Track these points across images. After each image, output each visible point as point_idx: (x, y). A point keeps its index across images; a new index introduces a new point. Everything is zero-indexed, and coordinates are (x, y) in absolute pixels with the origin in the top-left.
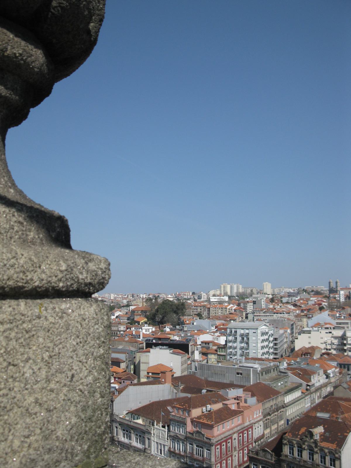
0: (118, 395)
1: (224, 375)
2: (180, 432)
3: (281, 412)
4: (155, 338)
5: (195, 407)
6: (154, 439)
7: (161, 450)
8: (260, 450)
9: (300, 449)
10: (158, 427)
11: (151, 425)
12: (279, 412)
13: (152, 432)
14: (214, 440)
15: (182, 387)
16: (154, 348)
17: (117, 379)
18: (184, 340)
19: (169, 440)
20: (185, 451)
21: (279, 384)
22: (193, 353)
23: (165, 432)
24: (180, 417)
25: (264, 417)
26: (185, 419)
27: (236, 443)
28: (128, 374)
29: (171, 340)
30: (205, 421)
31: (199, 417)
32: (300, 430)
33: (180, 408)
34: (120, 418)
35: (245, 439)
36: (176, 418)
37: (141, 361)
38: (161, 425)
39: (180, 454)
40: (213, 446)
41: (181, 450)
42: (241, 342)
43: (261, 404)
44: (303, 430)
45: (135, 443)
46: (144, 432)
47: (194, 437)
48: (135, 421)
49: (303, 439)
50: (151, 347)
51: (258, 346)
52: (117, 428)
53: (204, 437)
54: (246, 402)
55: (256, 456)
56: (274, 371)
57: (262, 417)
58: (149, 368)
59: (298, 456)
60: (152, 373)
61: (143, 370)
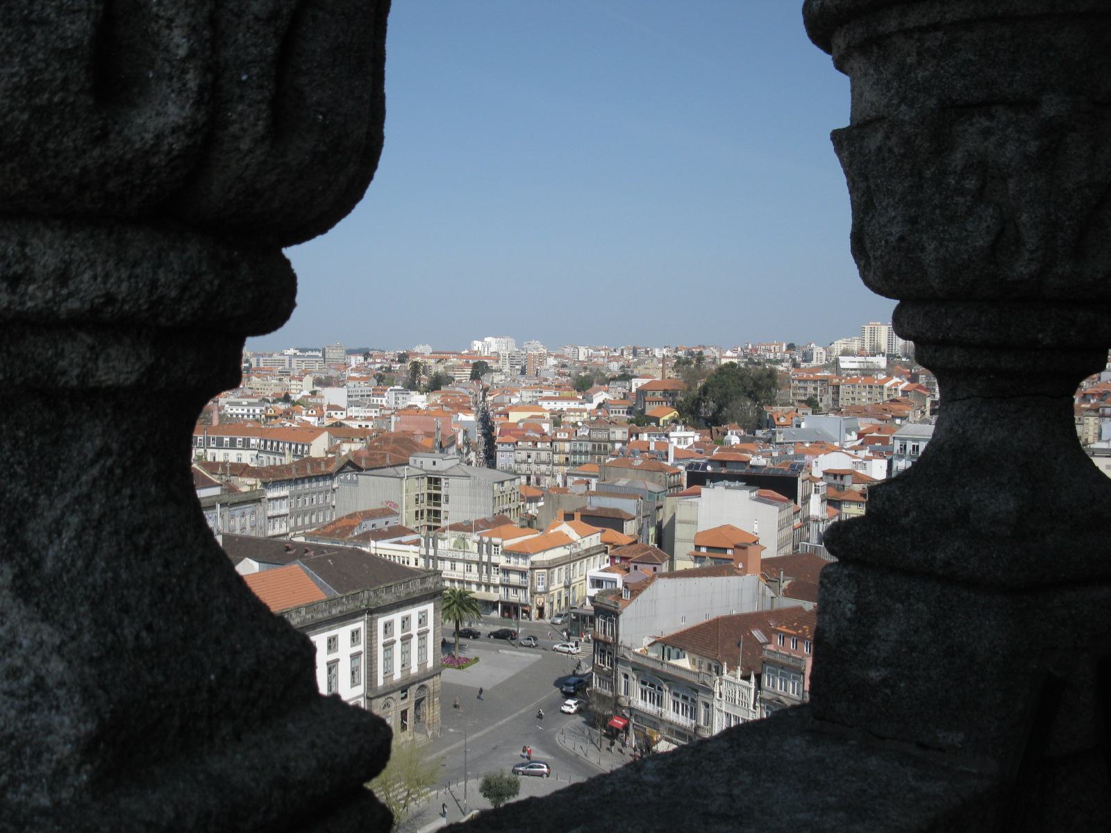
4: (711, 462)
10: (732, 679)
11: (715, 674)
13: (717, 690)
15: (787, 583)
17: (617, 561)
18: (786, 468)
19: (758, 710)
22: (806, 499)
23: (749, 689)
24: (789, 656)
26: (801, 660)
28: (647, 549)
29: (752, 467)
33: (790, 635)
34: (636, 654)
37: (678, 517)
38: (739, 673)
46: (695, 689)
48: (673, 662)
50: (703, 484)
52: (626, 676)
61: (682, 540)
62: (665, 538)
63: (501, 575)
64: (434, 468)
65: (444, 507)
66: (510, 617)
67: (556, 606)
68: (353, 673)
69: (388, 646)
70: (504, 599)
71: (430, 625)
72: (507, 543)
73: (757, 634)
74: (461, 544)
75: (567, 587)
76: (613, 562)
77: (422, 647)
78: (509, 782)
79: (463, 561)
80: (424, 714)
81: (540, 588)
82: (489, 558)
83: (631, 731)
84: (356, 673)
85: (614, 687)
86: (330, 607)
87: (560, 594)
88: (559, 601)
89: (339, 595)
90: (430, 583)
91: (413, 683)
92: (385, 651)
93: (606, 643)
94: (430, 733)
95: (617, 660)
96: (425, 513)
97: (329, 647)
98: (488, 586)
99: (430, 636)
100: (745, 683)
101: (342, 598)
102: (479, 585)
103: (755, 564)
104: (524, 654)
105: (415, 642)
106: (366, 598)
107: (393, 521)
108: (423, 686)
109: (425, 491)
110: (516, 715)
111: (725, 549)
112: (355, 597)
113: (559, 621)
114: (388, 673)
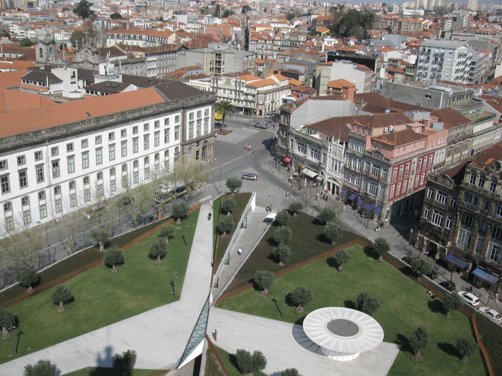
0: (296, 109)
1: (411, 96)
2: (358, 150)
3: (467, 141)
4: (338, 51)
5: (377, 126)
6: (330, 155)
7: (336, 166)
8: (440, 176)
9: (482, 179)
10: (335, 144)
12: (465, 141)
13: (329, 148)
14: (392, 162)
15: (364, 105)
16: (337, 61)
17: (294, 92)
18: (371, 56)
19: (346, 157)
20: (361, 170)
21: (471, 112)
22: (379, 70)
23: (342, 148)
24: (360, 135)
25: (449, 144)
26: (365, 137)
27: (414, 167)
28: (307, 88)
29: (356, 54)
30: (386, 142)
31: (380, 137)
32: (486, 160)
34: (297, 131)
35: (425, 164)
36: (355, 136)
37: (322, 75)
38: (339, 141)
39: (355, 172)
40: (391, 166)
41: (357, 168)
42: (434, 63)
43: (447, 130)
44: (490, 161)
45: (310, 158)
46: (320, 147)
47: (372, 156)
48: (311, 135)
49: (488, 169)
50: (334, 61)
51: (452, 69)
52: (292, 141)
53: (382, 157)
54: (431, 126)
55: (434, 181)
56: (467, 97)
57: (446, 144)
58: (330, 82)
59: (479, 185)
60: (333, 88)
61: (323, 85)
62: (316, 84)
63: (244, 96)
64: (219, 49)
65: (222, 66)
66: (247, 114)
67: (267, 110)
68: (176, 134)
69: (191, 123)
70: (245, 106)
71: (210, 115)
72: (248, 82)
73: (348, 125)
74: (228, 82)
75: (272, 102)
76: (292, 92)
77: (206, 124)
78: (238, 182)
79: (228, 89)
80: (206, 153)
81: (261, 102)
82: (240, 89)
83: (293, 164)
84: (177, 134)
85: (287, 145)
86: (166, 106)
87: (269, 105)
88: (269, 108)
89: (170, 101)
90: (210, 97)
91: (202, 140)
92: (190, 125)
93: (285, 126)
94: (209, 161)
95: (289, 133)
96: (214, 69)
97: (166, 123)
98: (239, 101)
99: (210, 120)
100: (341, 146)
101: (171, 102)
102: (235, 100)
103: (351, 95)
104: (251, 130)
105: (203, 122)
106: (181, 103)
107: (200, 72)
108: (206, 141)
109: (214, 59)
110: (245, 155)
111: (340, 89)
112: (177, 102)
113: (268, 117)
114: (191, 135)
